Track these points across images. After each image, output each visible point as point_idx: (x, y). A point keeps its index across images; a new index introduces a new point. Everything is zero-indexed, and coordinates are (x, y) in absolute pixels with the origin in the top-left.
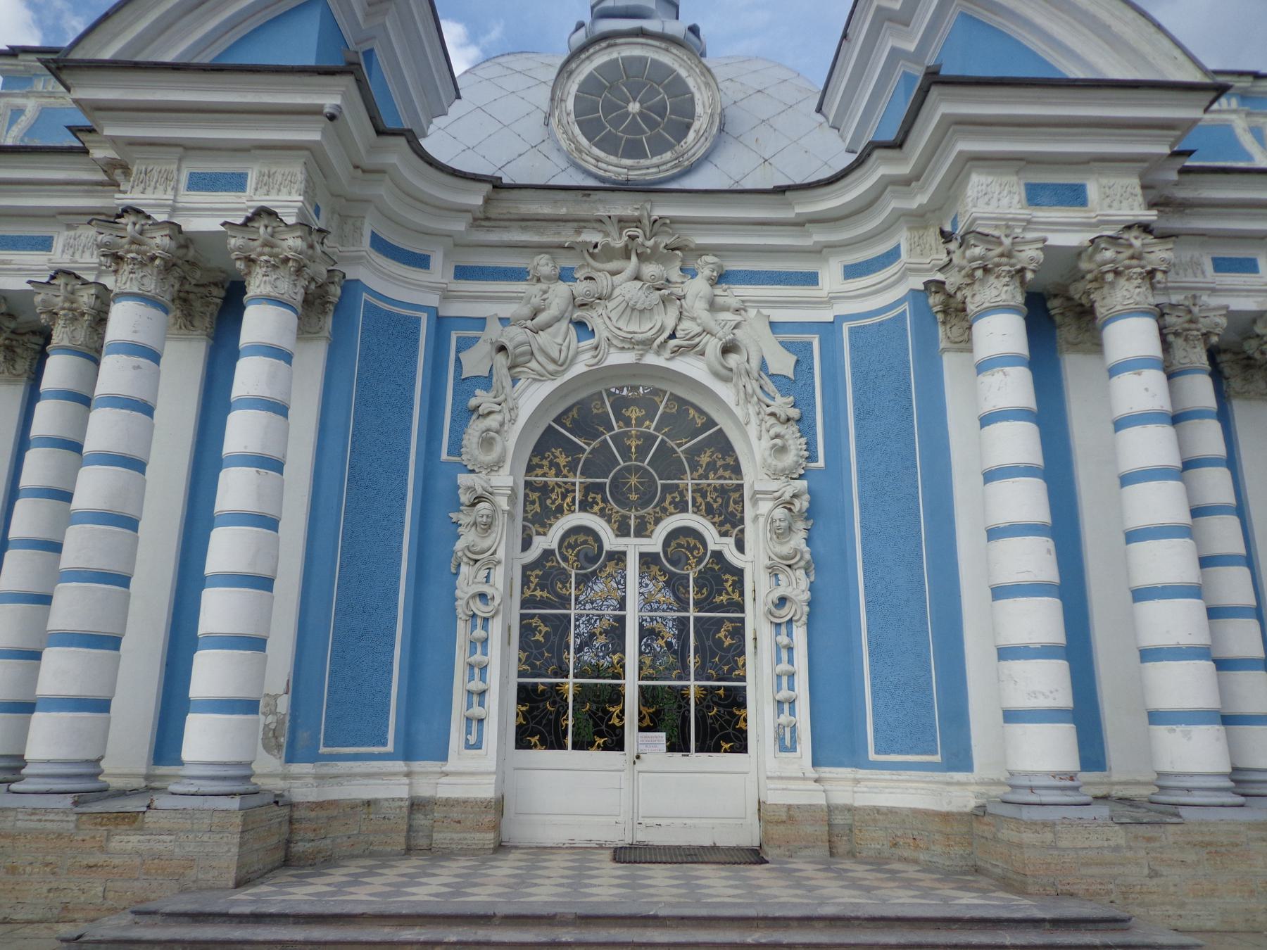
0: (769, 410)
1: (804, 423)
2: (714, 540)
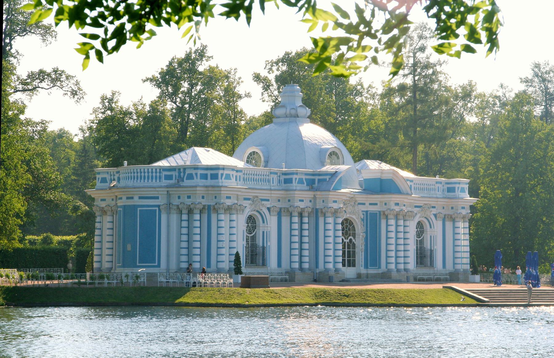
2: (353, 240)
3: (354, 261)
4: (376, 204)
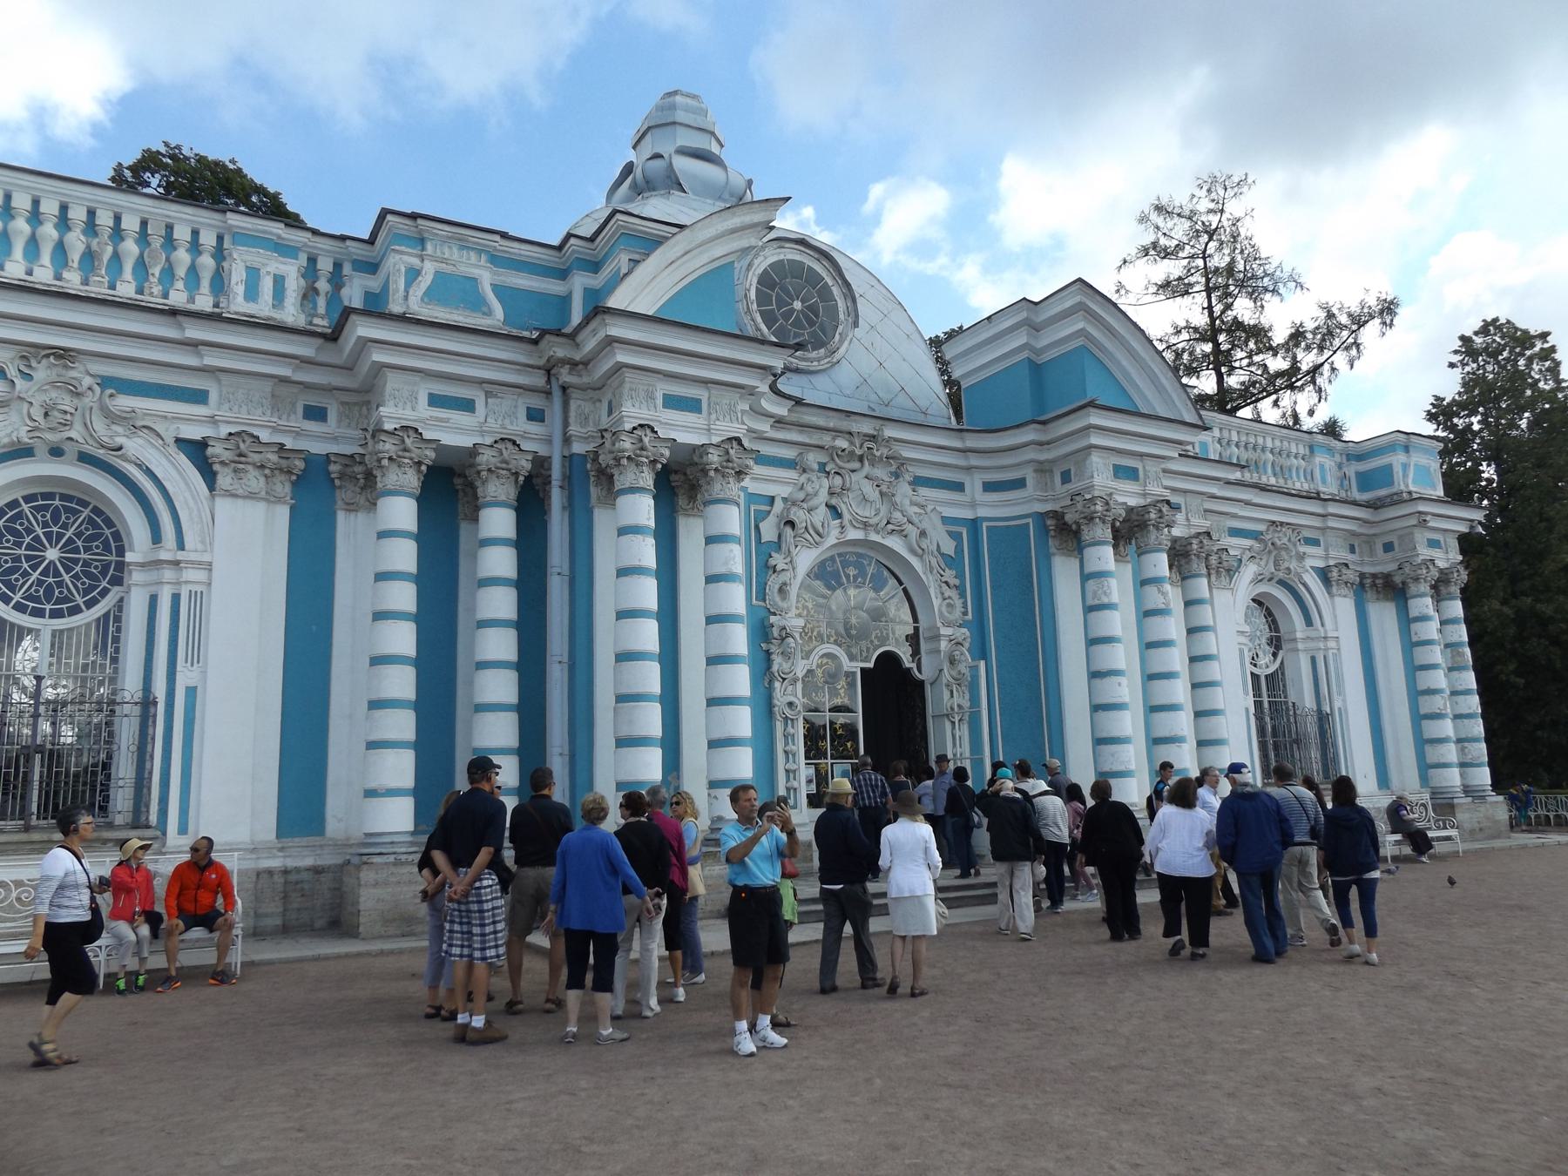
0: (944, 579)
1: (961, 590)
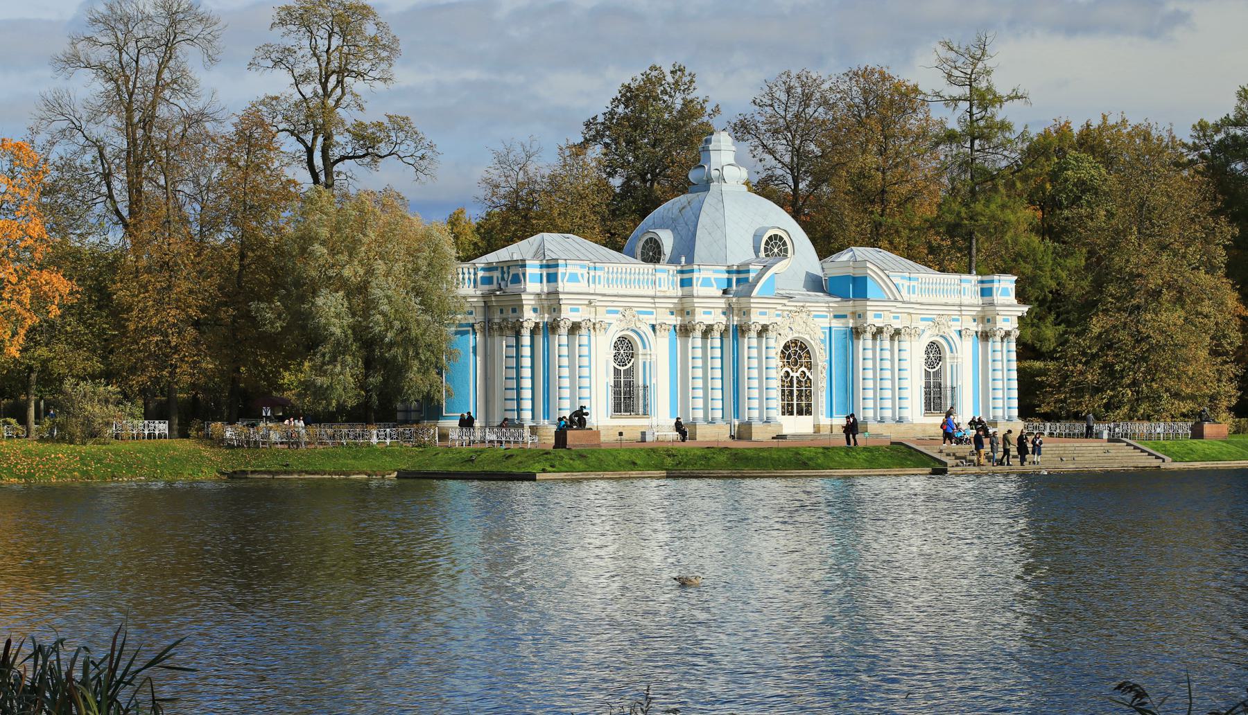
1: (825, 350)
2: (808, 374)
3: (810, 405)
4: (845, 316)
